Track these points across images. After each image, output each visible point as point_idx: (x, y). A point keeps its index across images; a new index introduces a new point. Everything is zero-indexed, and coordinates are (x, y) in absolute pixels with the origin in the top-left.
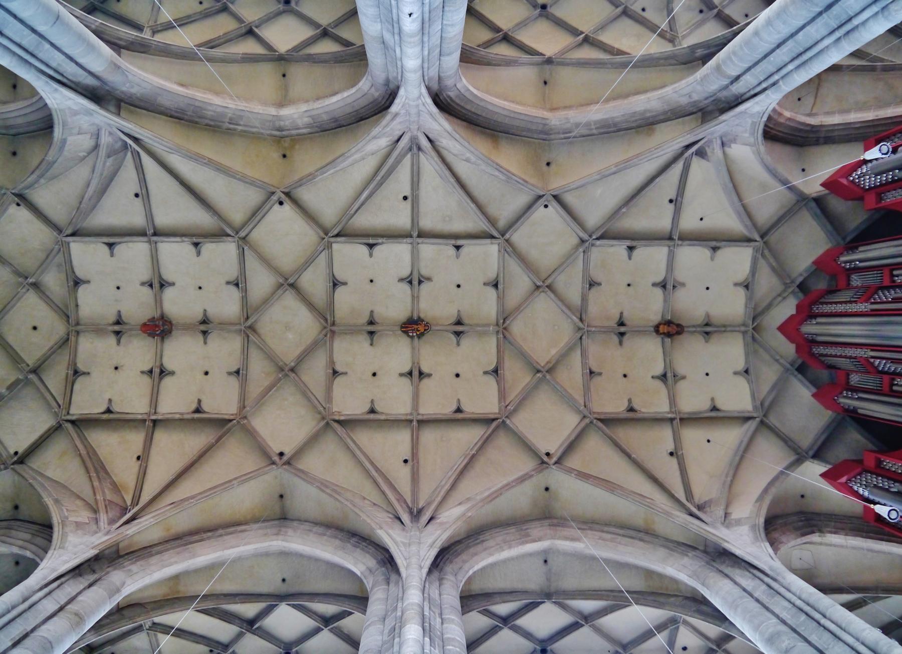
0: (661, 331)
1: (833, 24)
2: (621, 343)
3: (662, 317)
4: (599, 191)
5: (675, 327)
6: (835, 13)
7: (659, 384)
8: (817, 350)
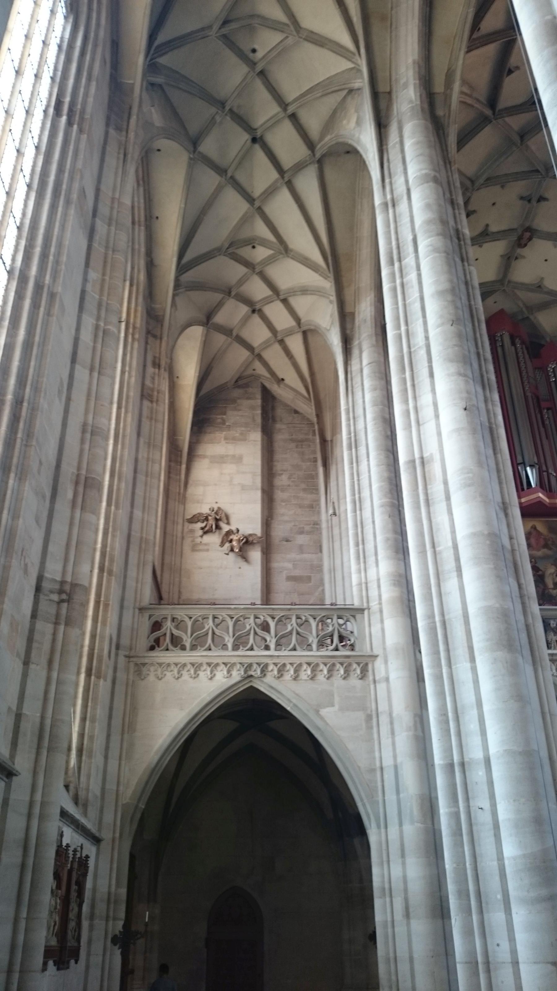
2: (522, 198)
5: (525, 242)
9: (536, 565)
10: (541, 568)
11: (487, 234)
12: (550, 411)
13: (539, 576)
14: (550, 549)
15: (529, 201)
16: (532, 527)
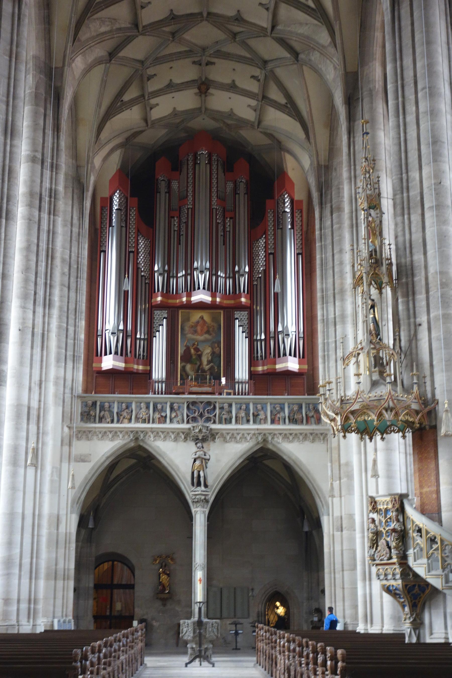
7: (166, 82)
8: (191, 157)
9: (198, 347)
10: (201, 349)
11: (172, 86)
12: (231, 220)
14: (210, 334)
15: (200, 65)
16: (200, 317)
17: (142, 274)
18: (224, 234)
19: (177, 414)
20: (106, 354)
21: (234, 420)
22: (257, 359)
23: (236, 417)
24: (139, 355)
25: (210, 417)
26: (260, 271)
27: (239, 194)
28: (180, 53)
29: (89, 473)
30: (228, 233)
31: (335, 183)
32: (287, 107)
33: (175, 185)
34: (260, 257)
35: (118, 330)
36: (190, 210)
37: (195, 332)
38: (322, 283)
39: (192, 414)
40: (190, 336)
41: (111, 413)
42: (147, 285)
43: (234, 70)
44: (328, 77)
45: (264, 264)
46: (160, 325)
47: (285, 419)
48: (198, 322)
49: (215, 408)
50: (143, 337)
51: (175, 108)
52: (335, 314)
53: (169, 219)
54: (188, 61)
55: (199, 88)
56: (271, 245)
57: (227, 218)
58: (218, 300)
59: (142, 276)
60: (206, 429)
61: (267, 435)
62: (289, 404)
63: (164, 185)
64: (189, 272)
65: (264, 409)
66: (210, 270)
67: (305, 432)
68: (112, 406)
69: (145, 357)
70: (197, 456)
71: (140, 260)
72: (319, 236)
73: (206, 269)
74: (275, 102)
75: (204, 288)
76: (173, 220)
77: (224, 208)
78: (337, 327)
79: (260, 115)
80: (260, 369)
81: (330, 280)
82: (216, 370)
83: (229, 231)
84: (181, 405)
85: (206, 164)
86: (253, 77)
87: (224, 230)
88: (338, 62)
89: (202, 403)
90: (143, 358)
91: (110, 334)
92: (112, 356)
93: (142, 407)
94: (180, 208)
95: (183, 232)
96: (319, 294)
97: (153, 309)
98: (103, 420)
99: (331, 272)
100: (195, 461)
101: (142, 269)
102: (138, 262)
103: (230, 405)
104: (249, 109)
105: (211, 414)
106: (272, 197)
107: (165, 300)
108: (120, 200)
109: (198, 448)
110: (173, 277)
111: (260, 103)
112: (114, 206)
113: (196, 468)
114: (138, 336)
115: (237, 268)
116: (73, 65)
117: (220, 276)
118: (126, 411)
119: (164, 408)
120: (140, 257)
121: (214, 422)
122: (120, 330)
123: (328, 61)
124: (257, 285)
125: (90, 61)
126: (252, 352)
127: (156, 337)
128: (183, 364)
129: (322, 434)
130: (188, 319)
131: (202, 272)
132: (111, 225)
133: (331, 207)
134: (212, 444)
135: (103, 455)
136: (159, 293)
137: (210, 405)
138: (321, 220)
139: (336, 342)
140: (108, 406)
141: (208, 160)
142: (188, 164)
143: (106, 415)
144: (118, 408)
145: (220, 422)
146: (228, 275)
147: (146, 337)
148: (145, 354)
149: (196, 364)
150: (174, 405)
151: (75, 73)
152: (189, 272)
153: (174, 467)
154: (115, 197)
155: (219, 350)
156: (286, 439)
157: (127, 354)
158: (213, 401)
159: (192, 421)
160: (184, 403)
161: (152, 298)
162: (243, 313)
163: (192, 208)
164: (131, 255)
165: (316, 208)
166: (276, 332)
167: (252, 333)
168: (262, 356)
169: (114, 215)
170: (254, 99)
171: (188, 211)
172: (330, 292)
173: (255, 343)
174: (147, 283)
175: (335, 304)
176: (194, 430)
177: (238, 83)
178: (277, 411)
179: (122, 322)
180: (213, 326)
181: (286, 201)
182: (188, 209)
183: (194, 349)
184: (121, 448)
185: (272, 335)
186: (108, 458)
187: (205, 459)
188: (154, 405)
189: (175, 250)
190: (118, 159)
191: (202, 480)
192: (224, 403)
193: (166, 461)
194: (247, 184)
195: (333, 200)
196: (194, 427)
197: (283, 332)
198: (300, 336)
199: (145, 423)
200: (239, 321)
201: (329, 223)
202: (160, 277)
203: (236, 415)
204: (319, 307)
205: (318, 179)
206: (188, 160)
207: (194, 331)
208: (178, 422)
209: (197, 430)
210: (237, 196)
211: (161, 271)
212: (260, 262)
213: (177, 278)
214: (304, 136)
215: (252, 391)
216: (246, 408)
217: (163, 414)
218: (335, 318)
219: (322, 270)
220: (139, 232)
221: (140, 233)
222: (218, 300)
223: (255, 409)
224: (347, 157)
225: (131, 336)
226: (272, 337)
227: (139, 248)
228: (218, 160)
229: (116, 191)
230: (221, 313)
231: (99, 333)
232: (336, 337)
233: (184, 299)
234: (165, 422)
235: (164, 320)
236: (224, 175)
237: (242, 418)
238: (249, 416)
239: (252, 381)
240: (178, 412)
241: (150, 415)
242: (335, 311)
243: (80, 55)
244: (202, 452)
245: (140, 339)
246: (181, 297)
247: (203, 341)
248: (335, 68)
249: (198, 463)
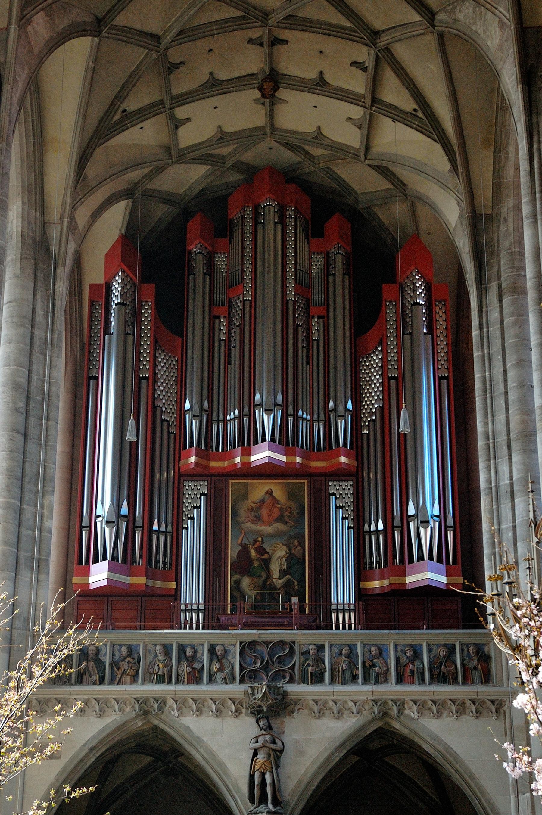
0: (265, 84)
1: (498, 440)
3: (282, 74)
4: (432, 67)
6: (504, 447)
12: (321, 320)
13: (263, 560)
14: (285, 523)
16: (267, 493)
17: (163, 418)
18: (308, 345)
19: (222, 665)
20: (96, 561)
21: (327, 675)
22: (371, 568)
23: (332, 670)
24: (157, 562)
25: (284, 671)
26: (374, 410)
27: (334, 275)
28: (225, 21)
29: (57, 780)
30: (315, 342)
31: (506, 243)
32: (417, 116)
33: (221, 261)
34: (373, 386)
35: (119, 516)
36: (247, 304)
37: (258, 519)
38: (486, 423)
39: (250, 666)
40: (248, 525)
41: (100, 664)
42: (172, 436)
43: (321, 52)
44: (489, 43)
45: (381, 397)
46: (194, 507)
47: (423, 674)
48: (263, 501)
49: (292, 651)
50: (163, 529)
51: (219, 127)
52: (511, 478)
53: (210, 319)
54: (239, 37)
55: (261, 89)
56: (392, 364)
57: (313, 317)
58: (298, 460)
59: (163, 421)
60: (276, 691)
61: (390, 703)
62: (429, 645)
63: (201, 262)
64: (246, 410)
65: (384, 654)
66: (284, 407)
67: (461, 698)
68: (103, 652)
69: (168, 566)
70: (259, 744)
71: (159, 392)
72: (478, 339)
73: (276, 405)
74: (396, 108)
75: (273, 440)
76: (217, 321)
77: (308, 300)
78: (517, 501)
79: (368, 135)
80: (376, 584)
81: (501, 417)
82: (297, 588)
83: (318, 341)
84: (230, 648)
85: (276, 223)
86: (354, 64)
87: (308, 337)
88: (507, 15)
89: (267, 643)
90: (164, 568)
91: (104, 523)
92: (106, 563)
93: (158, 652)
94: (230, 300)
95: (236, 342)
96: (481, 443)
97: (182, 479)
98: (85, 677)
99: (502, 402)
100: (255, 754)
101: (163, 409)
102: (156, 396)
103: (320, 648)
104: (349, 124)
105: (285, 666)
106: (394, 280)
107: (203, 462)
108: (122, 288)
109: (261, 730)
110: (218, 421)
111: (369, 111)
112: (114, 299)
113: (257, 767)
114: (155, 527)
115: (331, 404)
116: (30, 28)
117: (302, 418)
118: (128, 659)
119: (199, 654)
120: (159, 387)
121: (291, 680)
122: (124, 516)
123: (489, 14)
124: (368, 435)
125: (61, 27)
126: (362, 555)
127: (187, 528)
128: (237, 577)
129: (493, 702)
130: (245, 496)
131: (268, 411)
132: (107, 331)
133: (500, 287)
134: (287, 720)
135: (84, 745)
136: (193, 449)
137: (284, 649)
138: (480, 311)
139: (514, 527)
140: (94, 652)
141: (279, 217)
142: (243, 225)
143: (90, 669)
144: (113, 655)
145: (304, 681)
146: (315, 417)
147: (169, 529)
148: (168, 560)
149: (260, 576)
150: (217, 648)
151: (32, 43)
152: (246, 410)
153: (216, 766)
154: (114, 284)
155: (302, 551)
156: (426, 712)
157: (134, 561)
158: (288, 639)
159: (250, 678)
160: (235, 645)
161: (179, 460)
162: (344, 484)
163: (250, 301)
164: (144, 383)
165: (471, 290)
166: (405, 518)
167: (361, 518)
168: (379, 562)
169: (113, 315)
170: (358, 105)
171: (244, 306)
172: (502, 439)
173: (367, 538)
174: (172, 433)
175: (510, 459)
176: (253, 694)
177: (328, 78)
178: (408, 657)
179: (125, 503)
180: (290, 508)
181: (418, 285)
182: (244, 301)
183: (256, 550)
184: (117, 729)
185: (397, 522)
186: (92, 749)
187: (274, 750)
188: (179, 648)
189: (222, 371)
190: (120, 220)
191: (269, 789)
192: (310, 645)
193: (202, 756)
194: (347, 258)
195: (502, 274)
196: (252, 689)
197: (417, 516)
198: (448, 524)
199: (163, 682)
200: (336, 498)
201: (495, 315)
202: (194, 422)
203: (332, 665)
204: (482, 465)
205: (475, 238)
206: (243, 217)
207: (256, 517)
208: (225, 681)
209: (260, 696)
210: (331, 277)
211: (197, 408)
212: (373, 394)
213: (225, 422)
214: (449, 166)
215: (361, 622)
216: (351, 652)
217: (197, 666)
218: (512, 485)
219: (485, 400)
220: (156, 343)
221: (160, 346)
222: (298, 460)
223: (367, 654)
224: (528, 179)
225: (143, 527)
226: (396, 527)
227: (157, 371)
228: (296, 218)
229: (118, 273)
230: (304, 483)
231: (85, 522)
232: (514, 520)
233: (238, 460)
234: (198, 681)
235: (202, 497)
236: (308, 243)
237: (343, 671)
238: (357, 668)
239: (360, 603)
240: (224, 661)
241: (172, 666)
242: (511, 472)
243: (42, 13)
244: (268, 737)
245: (159, 532)
246: (233, 457)
247: (273, 536)
248: (502, 24)
249: (261, 757)
